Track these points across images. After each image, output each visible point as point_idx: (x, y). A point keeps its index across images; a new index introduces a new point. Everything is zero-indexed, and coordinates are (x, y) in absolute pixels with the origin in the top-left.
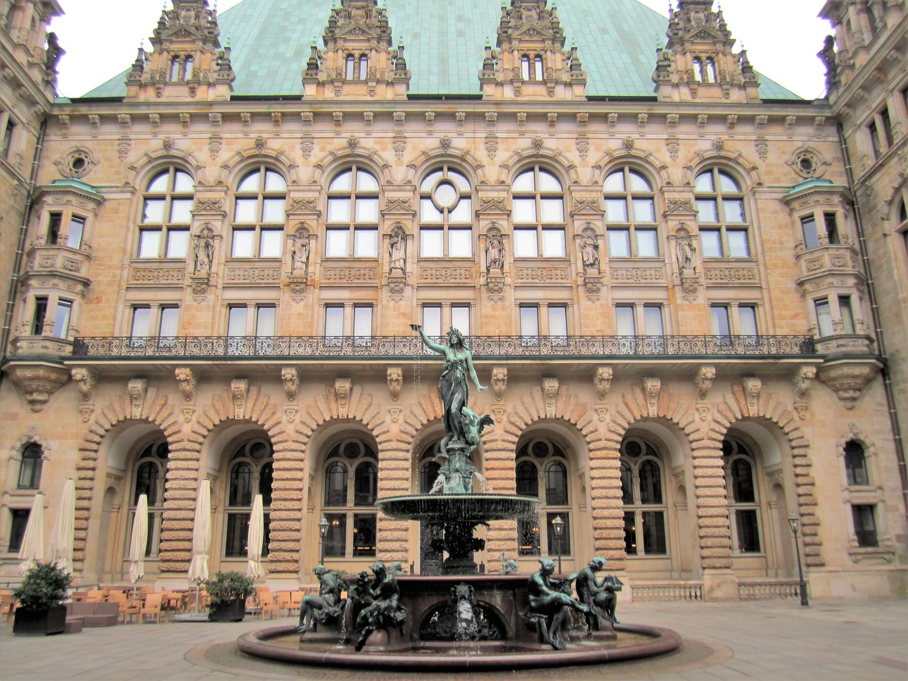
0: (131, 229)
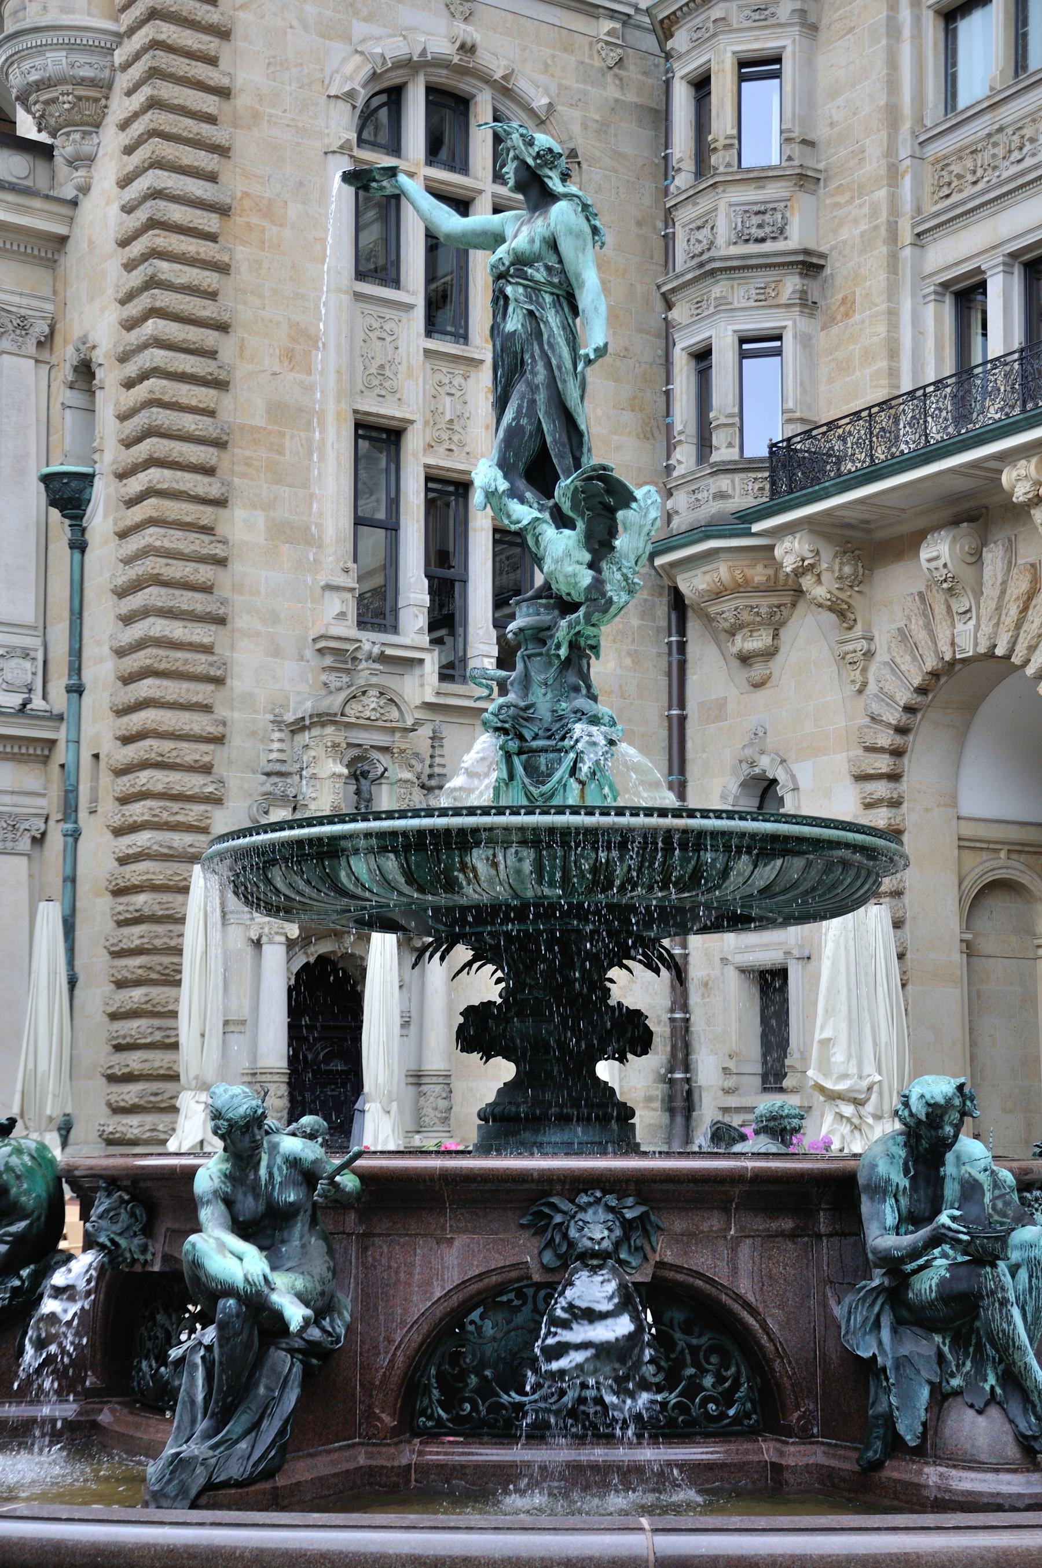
0: (907, 32)
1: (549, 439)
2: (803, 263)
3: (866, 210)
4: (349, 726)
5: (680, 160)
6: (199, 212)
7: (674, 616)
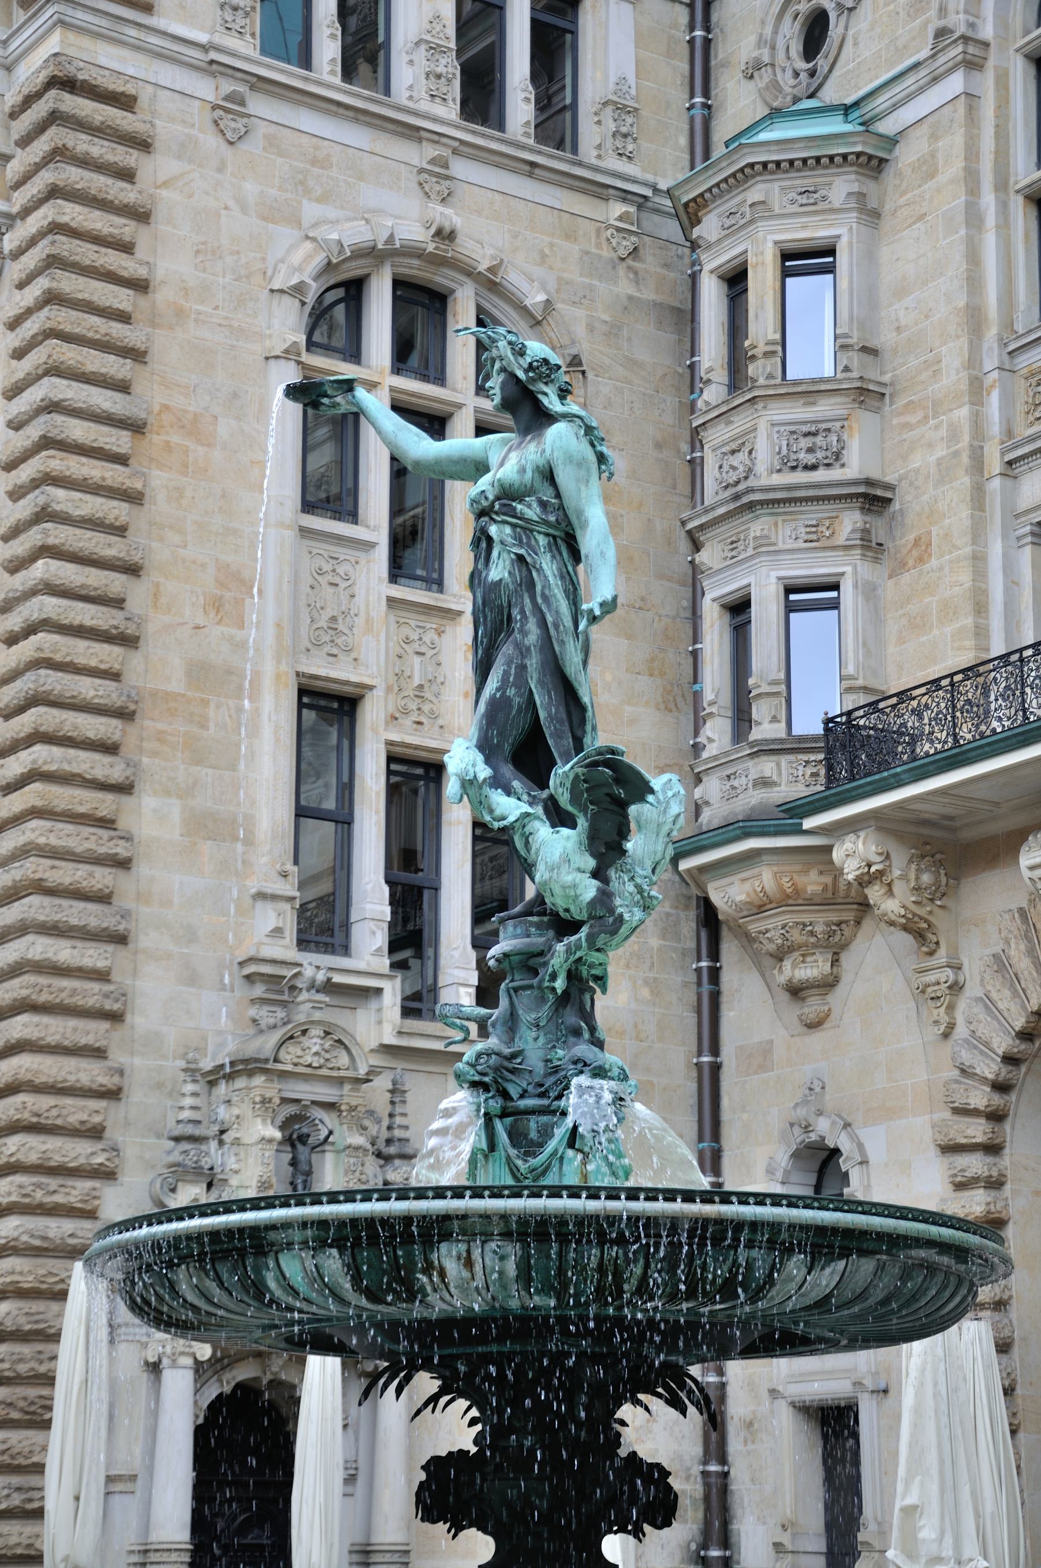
0: (991, 220)
1: (542, 715)
2: (865, 495)
3: (943, 432)
4: (283, 1075)
5: (710, 370)
6: (105, 429)
7: (704, 934)
